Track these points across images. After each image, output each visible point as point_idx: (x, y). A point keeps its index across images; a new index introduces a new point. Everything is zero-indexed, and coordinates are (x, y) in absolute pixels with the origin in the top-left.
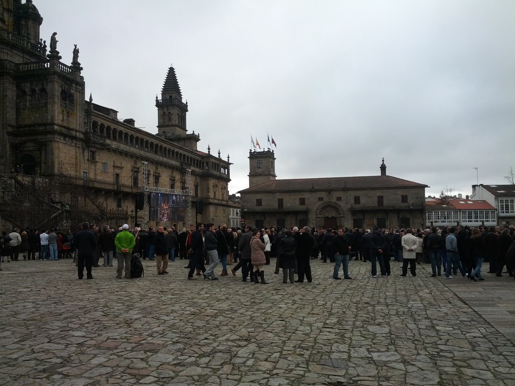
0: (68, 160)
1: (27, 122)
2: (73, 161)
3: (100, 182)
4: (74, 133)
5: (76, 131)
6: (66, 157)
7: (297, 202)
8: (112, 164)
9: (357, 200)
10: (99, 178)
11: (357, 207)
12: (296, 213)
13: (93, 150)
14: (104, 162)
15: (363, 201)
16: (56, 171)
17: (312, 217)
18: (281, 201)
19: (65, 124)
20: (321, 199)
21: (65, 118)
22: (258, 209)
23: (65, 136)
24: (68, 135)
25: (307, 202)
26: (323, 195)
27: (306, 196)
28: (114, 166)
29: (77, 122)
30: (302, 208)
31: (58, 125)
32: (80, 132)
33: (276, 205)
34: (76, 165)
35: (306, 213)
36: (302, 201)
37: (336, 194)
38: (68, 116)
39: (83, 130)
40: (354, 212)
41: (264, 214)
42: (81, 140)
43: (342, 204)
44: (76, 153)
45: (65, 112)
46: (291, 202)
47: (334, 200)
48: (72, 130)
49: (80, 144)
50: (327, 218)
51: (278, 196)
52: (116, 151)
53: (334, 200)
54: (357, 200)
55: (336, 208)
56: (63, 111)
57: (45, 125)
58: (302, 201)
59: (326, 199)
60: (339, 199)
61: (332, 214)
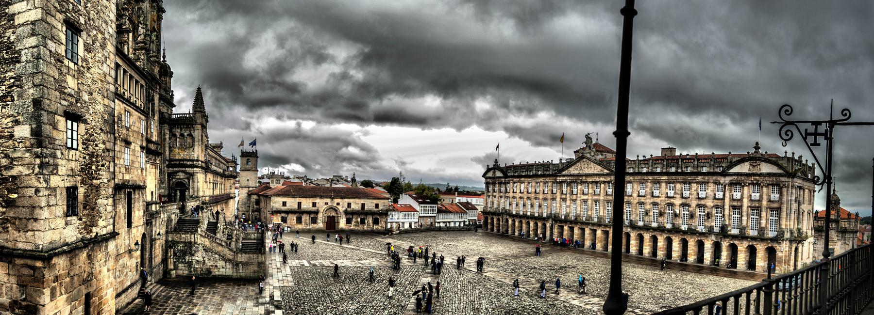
1: (177, 157)
7: (311, 205)
9: (349, 205)
12: (309, 213)
15: (353, 206)
17: (320, 215)
18: (299, 204)
20: (326, 204)
22: (284, 208)
26: (328, 200)
27: (318, 201)
33: (296, 207)
35: (317, 212)
36: (314, 204)
40: (346, 212)
41: (288, 212)
43: (339, 207)
47: (335, 205)
50: (329, 217)
53: (335, 205)
54: (349, 205)
55: (336, 210)
57: (193, 161)
58: (314, 204)
59: (330, 204)
60: (338, 204)
61: (333, 214)
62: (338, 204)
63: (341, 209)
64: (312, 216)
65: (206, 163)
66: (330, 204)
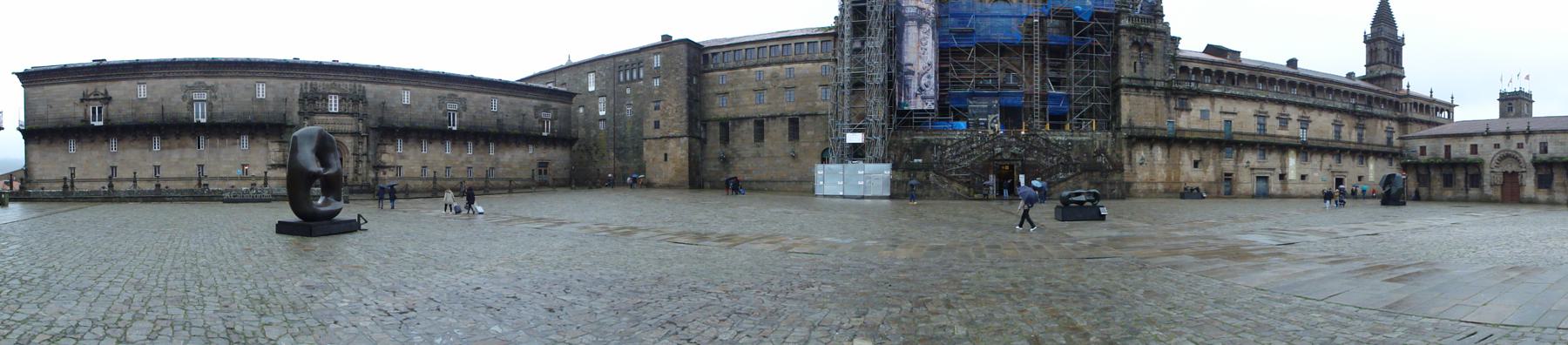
6: (1135, 109)
7: (1468, 150)
11: (1544, 157)
12: (1464, 164)
16: (1124, 122)
17: (1487, 170)
18: (1448, 148)
19: (1138, 75)
20: (1497, 146)
22: (1423, 159)
23: (1137, 88)
24: (1143, 86)
25: (1479, 150)
26: (1500, 140)
27: (1478, 141)
29: (1156, 71)
30: (1472, 157)
36: (1474, 149)
37: (1516, 140)
40: (1537, 164)
46: (1461, 150)
47: (1514, 147)
49: (1162, 93)
50: (1505, 173)
51: (1445, 142)
53: (1514, 147)
55: (1516, 159)
58: (1474, 149)
59: (1503, 146)
62: (1520, 146)
63: (1526, 156)
64: (1471, 172)
66: (1503, 146)
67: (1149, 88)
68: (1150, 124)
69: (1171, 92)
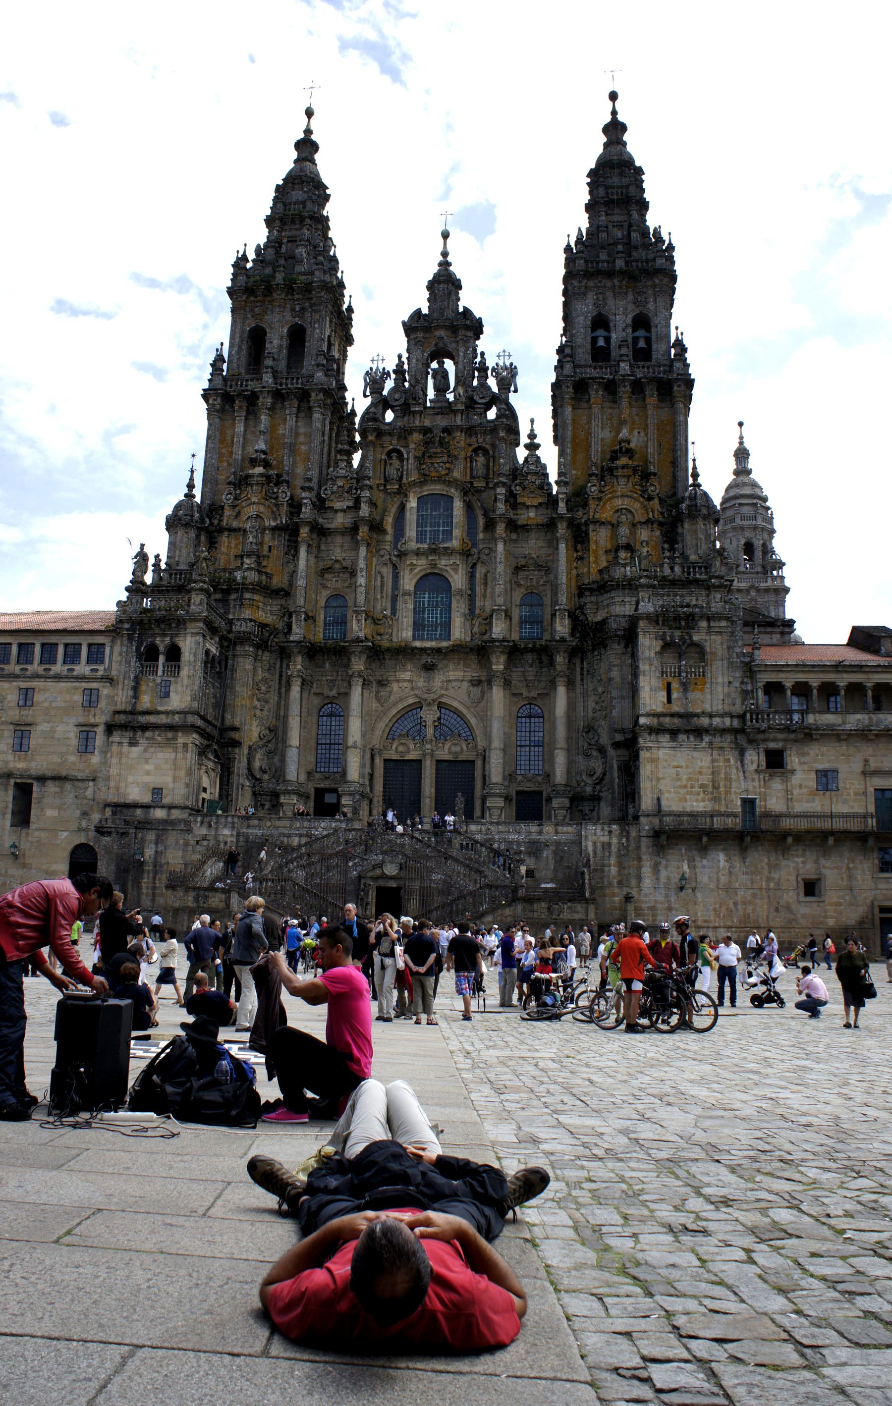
0: (689, 779)
2: (705, 779)
3: (805, 816)
4: (705, 721)
5: (711, 716)
8: (858, 767)
10: (800, 807)
13: (772, 745)
14: (821, 767)
19: (676, 708)
21: (675, 695)
23: (674, 733)
24: (684, 727)
28: (864, 773)
31: (647, 715)
32: (722, 716)
34: (716, 787)
38: (685, 690)
39: (738, 709)
42: (734, 731)
44: (713, 761)
45: (675, 685)
48: (697, 715)
52: (864, 735)
56: (669, 685)
65: (742, 717)
67: (699, 732)
68: (699, 804)
69: (742, 732)
